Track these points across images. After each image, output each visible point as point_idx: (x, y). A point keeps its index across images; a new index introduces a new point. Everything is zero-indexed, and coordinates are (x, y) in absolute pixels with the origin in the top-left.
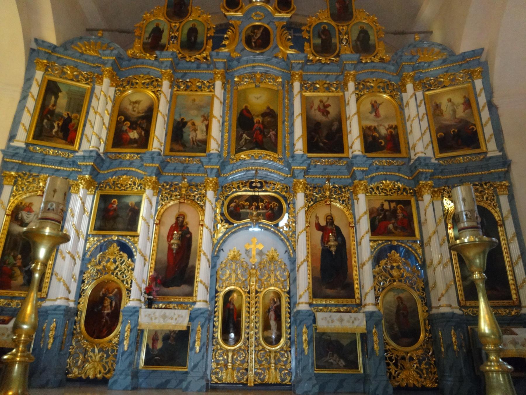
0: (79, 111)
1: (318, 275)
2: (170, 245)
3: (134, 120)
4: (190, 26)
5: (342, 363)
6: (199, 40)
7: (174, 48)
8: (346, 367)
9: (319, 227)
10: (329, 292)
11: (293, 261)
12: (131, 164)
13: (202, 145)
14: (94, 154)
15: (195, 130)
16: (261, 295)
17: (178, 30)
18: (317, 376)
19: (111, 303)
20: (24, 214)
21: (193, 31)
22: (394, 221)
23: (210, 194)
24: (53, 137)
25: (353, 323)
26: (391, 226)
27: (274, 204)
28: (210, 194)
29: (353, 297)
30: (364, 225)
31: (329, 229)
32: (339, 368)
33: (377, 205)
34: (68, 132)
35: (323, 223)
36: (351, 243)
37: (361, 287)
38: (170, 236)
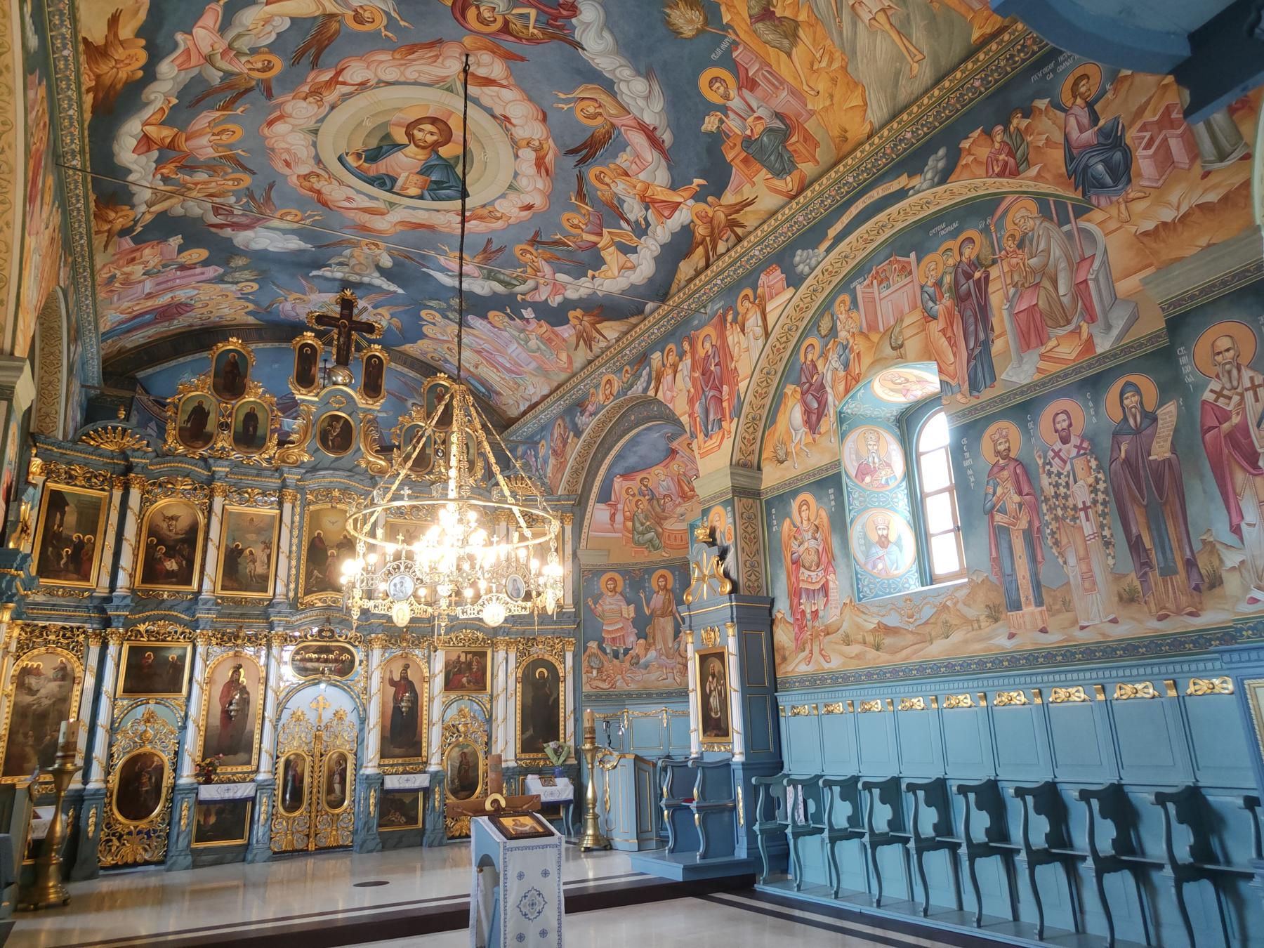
0: (94, 533)
1: (388, 735)
3: (172, 543)
4: (246, 410)
5: (403, 819)
6: (260, 432)
7: (223, 442)
8: (406, 823)
9: (392, 683)
10: (397, 751)
11: (363, 720)
12: (170, 608)
13: (261, 583)
14: (128, 601)
15: (254, 561)
16: (326, 759)
17: (230, 415)
18: (380, 834)
19: (150, 779)
20: (32, 681)
21: (251, 418)
22: (467, 675)
24: (62, 570)
25: (421, 781)
26: (464, 680)
27: (345, 656)
29: (420, 755)
30: (439, 681)
31: (404, 687)
32: (400, 825)
33: (454, 657)
34: (80, 563)
35: (397, 678)
36: (425, 700)
37: (429, 745)
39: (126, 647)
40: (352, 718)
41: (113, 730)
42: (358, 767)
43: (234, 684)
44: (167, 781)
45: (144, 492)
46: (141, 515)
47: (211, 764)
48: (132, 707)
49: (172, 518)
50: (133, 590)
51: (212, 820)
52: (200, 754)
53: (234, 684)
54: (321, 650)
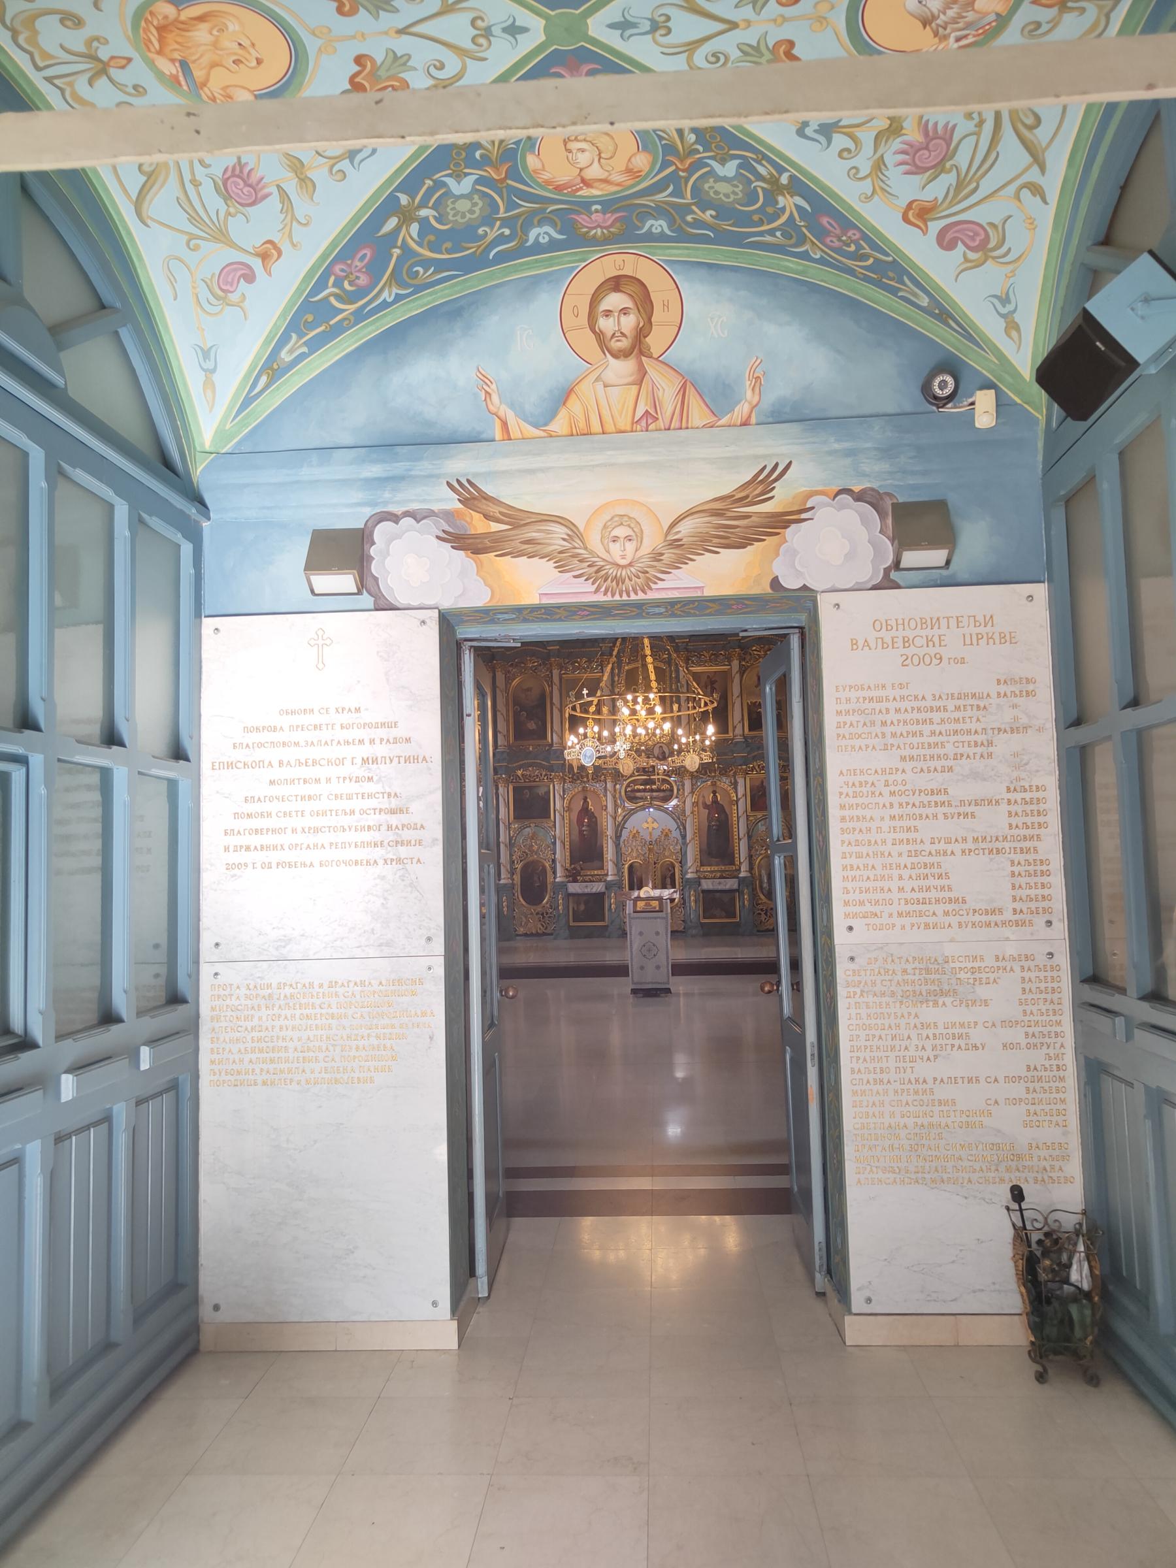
2: (581, 832)
5: (724, 914)
9: (706, 806)
10: (714, 860)
11: (684, 837)
16: (658, 866)
18: (702, 925)
23: (610, 785)
25: (731, 884)
28: (610, 785)
38: (580, 822)
39: (511, 787)
40: (676, 834)
41: (511, 845)
42: (683, 873)
43: (585, 811)
44: (550, 878)
45: (507, 673)
46: (507, 690)
47: (574, 869)
48: (521, 829)
49: (529, 690)
50: (509, 746)
51: (582, 907)
52: (568, 861)
53: (585, 811)
54: (645, 783)
